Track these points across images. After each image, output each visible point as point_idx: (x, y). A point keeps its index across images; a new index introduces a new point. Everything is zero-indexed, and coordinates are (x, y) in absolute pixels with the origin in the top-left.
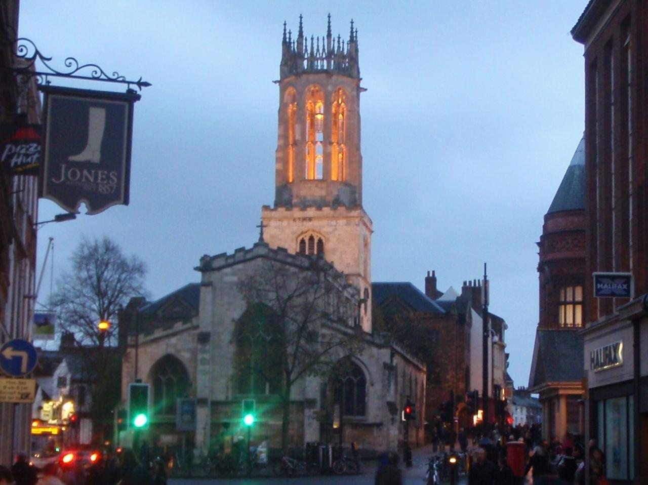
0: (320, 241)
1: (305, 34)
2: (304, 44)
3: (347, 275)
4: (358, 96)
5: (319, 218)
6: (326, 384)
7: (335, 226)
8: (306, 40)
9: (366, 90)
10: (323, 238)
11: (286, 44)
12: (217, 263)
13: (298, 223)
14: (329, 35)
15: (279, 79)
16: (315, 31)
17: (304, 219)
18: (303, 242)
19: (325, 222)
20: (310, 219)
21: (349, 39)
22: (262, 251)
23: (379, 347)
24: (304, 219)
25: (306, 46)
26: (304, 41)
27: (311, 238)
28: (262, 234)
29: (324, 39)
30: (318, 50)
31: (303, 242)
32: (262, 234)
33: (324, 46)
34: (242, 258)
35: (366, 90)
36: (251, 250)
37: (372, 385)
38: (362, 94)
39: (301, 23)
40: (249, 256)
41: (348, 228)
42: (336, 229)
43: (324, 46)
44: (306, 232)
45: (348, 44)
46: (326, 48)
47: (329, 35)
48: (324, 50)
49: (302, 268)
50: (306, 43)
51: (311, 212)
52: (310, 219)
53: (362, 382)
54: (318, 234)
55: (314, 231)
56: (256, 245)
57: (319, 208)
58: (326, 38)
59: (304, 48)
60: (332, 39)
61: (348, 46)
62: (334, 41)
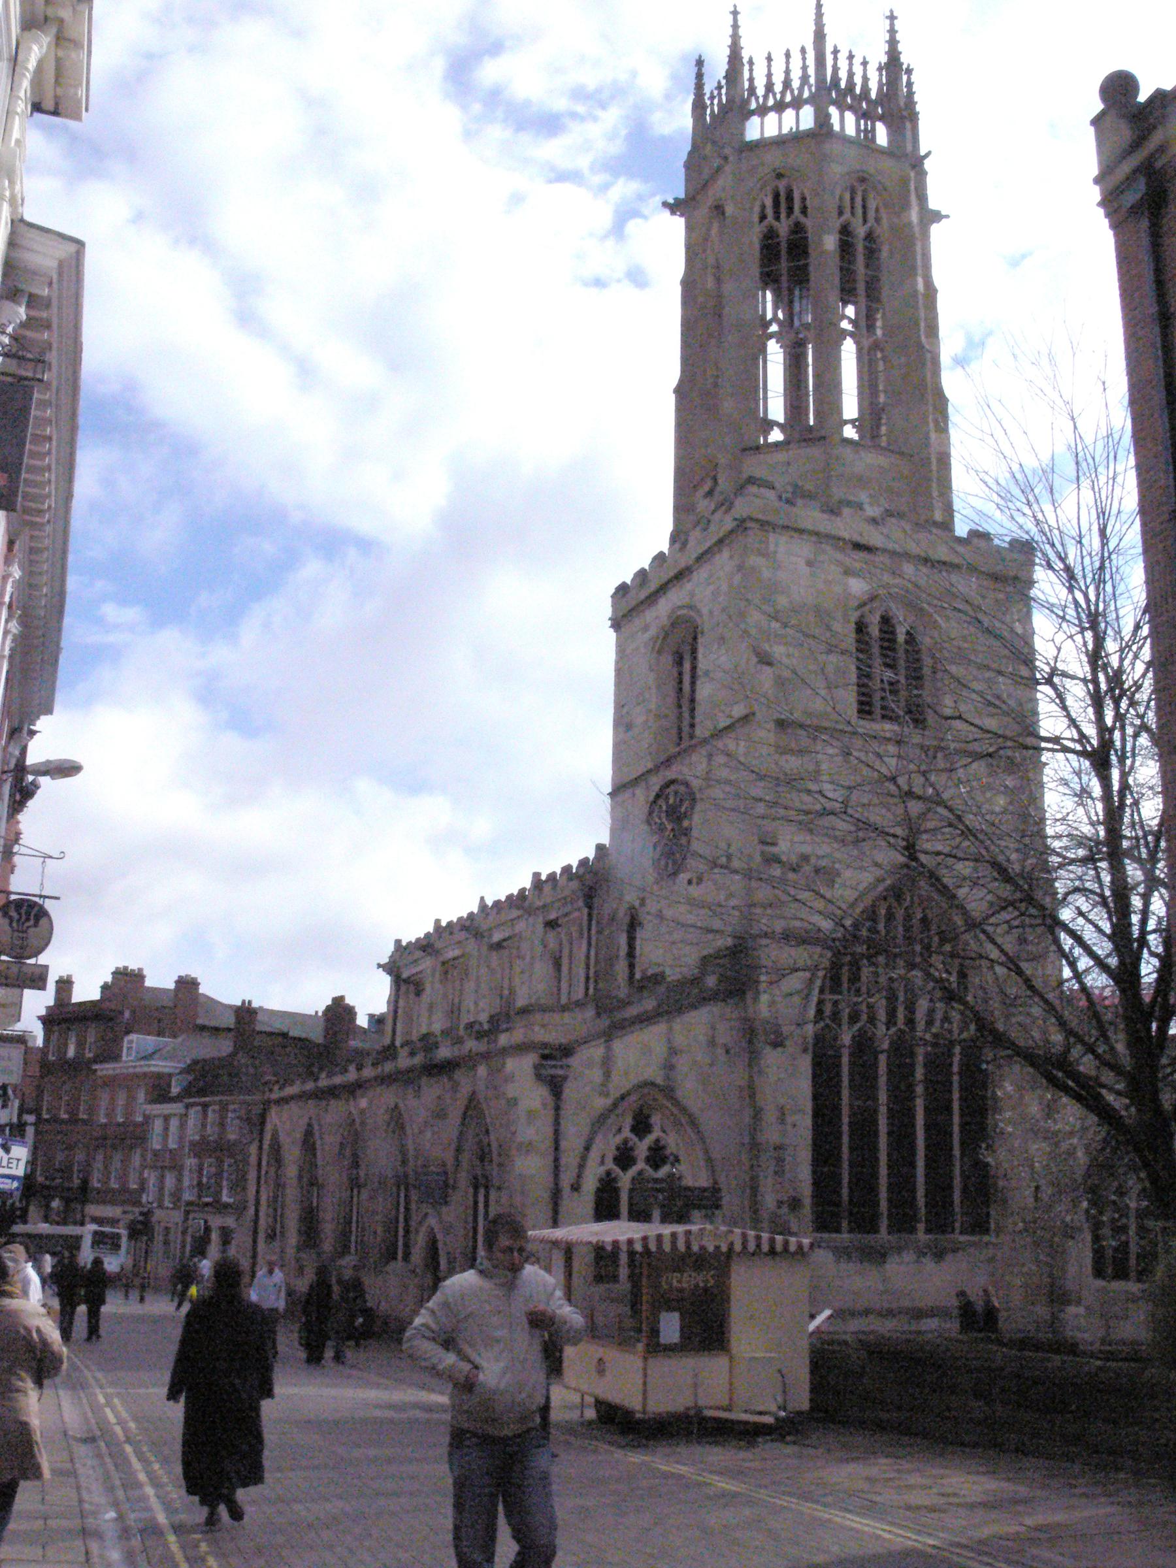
2: (746, 75)
8: (751, 63)
11: (699, 106)
14: (820, 36)
15: (682, 195)
21: (884, 59)
25: (751, 80)
26: (746, 68)
30: (787, 84)
33: (804, 68)
39: (735, 26)
43: (804, 68)
45: (880, 69)
46: (811, 71)
47: (820, 36)
48: (805, 78)
50: (751, 70)
59: (746, 85)
60: (829, 49)
61: (881, 75)
62: (836, 52)
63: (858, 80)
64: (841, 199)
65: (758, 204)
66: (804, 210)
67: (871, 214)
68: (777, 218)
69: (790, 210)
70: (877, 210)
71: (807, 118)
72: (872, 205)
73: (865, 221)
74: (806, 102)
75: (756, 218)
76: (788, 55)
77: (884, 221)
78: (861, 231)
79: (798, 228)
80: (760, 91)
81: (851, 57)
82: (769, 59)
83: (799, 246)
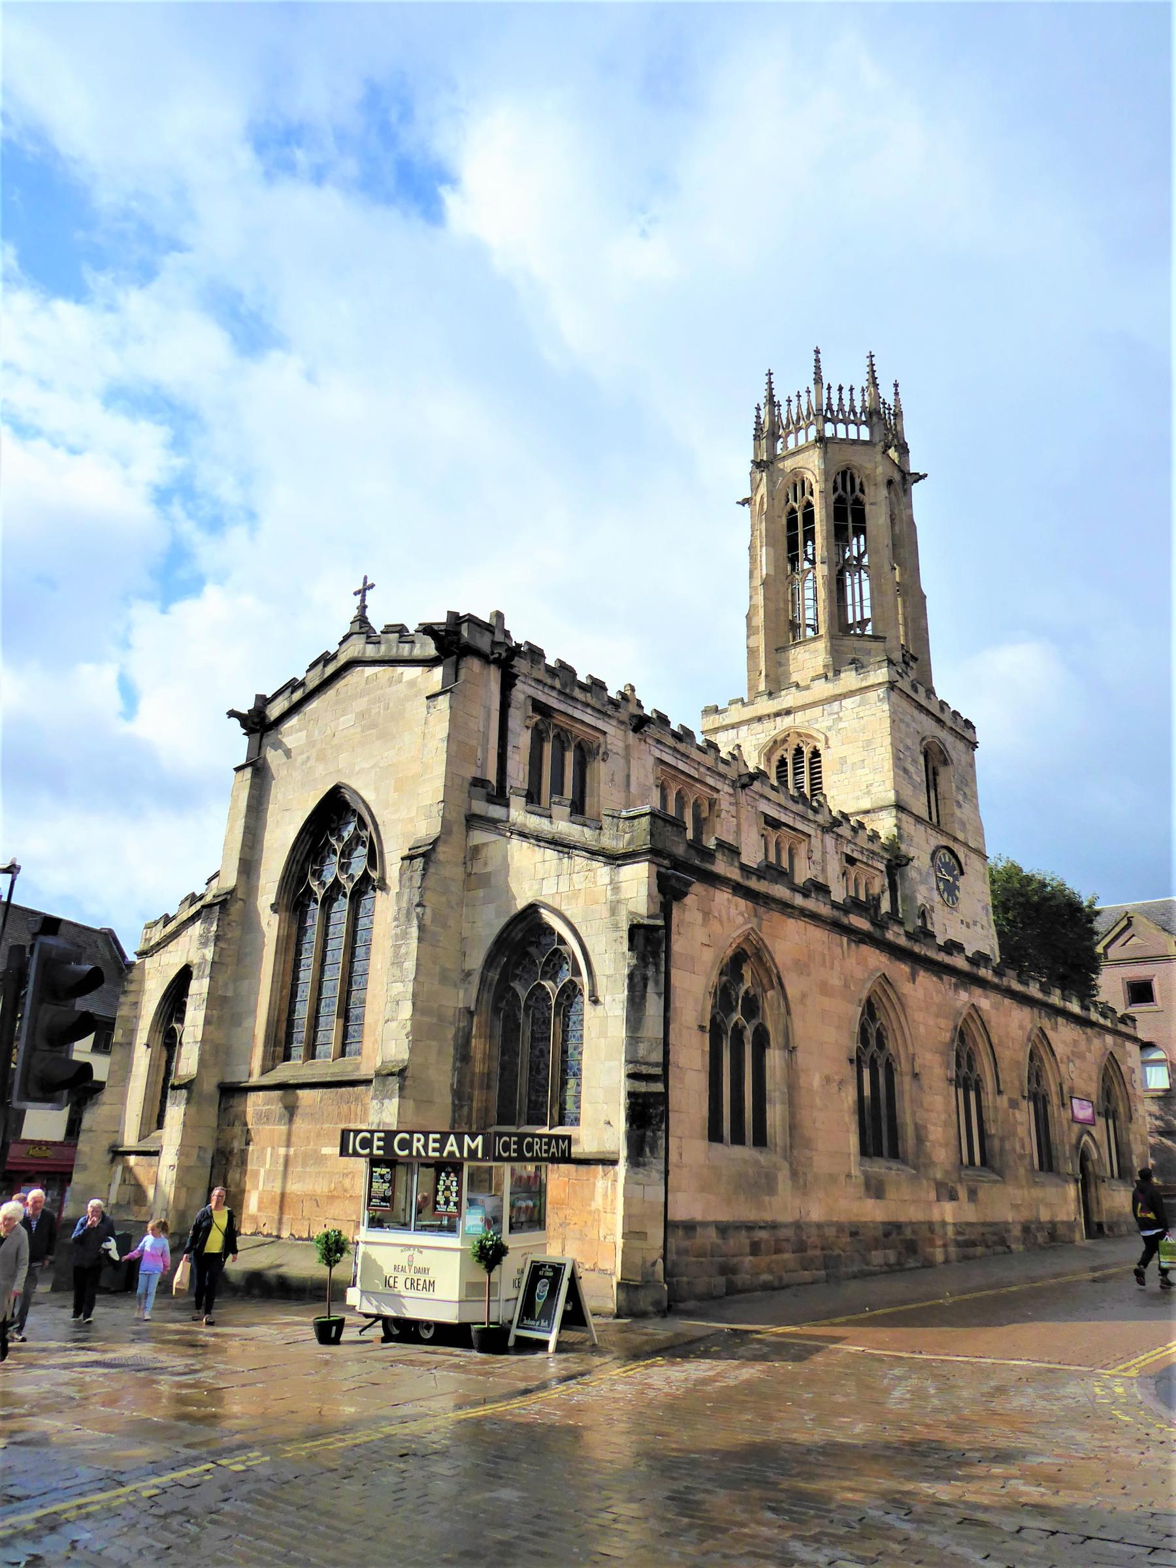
0: (816, 754)
1: (776, 399)
3: (867, 812)
4: (907, 492)
5: (804, 707)
6: (471, 1014)
7: (837, 713)
9: (926, 475)
10: (820, 746)
12: (274, 711)
13: (768, 724)
14: (818, 380)
15: (748, 495)
16: (793, 385)
17: (778, 714)
18: (783, 762)
19: (818, 710)
20: (788, 712)
22: (357, 647)
23: (615, 859)
24: (778, 714)
25: (780, 414)
27: (799, 752)
28: (363, 608)
29: (808, 392)
31: (783, 762)
32: (363, 608)
34: (317, 682)
35: (926, 475)
36: (335, 656)
37: (595, 1002)
38: (916, 488)
40: (331, 669)
41: (864, 711)
42: (840, 719)
43: (809, 402)
44: (785, 741)
45: (863, 390)
49: (429, 663)
51: (788, 699)
52: (788, 712)
53: (570, 992)
54: (809, 741)
55: (799, 735)
56: (346, 638)
57: (807, 688)
58: (812, 388)
62: (829, 388)
63: (846, 402)
64: (835, 482)
65: (784, 494)
66: (812, 494)
67: (857, 487)
68: (796, 501)
69: (803, 494)
70: (861, 484)
71: (812, 433)
72: (857, 481)
73: (853, 490)
74: (811, 424)
75: (783, 502)
76: (799, 396)
77: (866, 491)
78: (850, 501)
79: (809, 505)
80: (785, 422)
81: (840, 389)
82: (789, 401)
83: (809, 517)
